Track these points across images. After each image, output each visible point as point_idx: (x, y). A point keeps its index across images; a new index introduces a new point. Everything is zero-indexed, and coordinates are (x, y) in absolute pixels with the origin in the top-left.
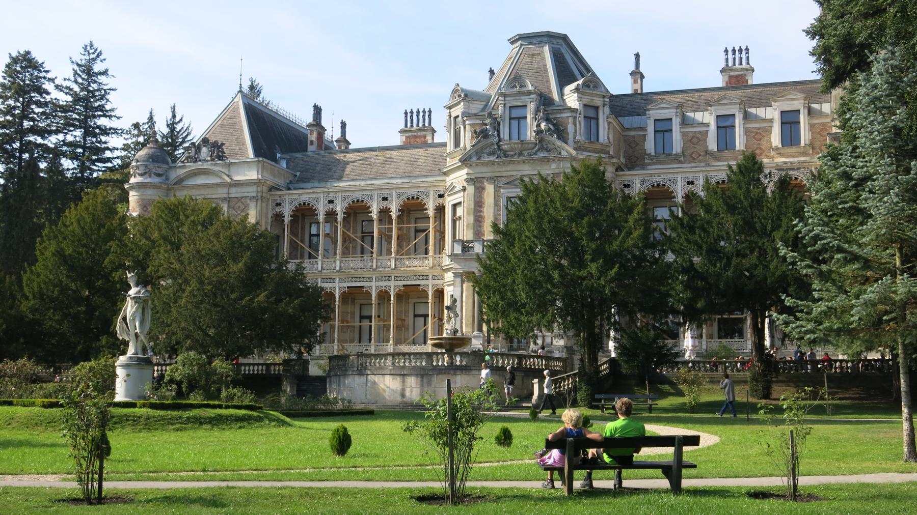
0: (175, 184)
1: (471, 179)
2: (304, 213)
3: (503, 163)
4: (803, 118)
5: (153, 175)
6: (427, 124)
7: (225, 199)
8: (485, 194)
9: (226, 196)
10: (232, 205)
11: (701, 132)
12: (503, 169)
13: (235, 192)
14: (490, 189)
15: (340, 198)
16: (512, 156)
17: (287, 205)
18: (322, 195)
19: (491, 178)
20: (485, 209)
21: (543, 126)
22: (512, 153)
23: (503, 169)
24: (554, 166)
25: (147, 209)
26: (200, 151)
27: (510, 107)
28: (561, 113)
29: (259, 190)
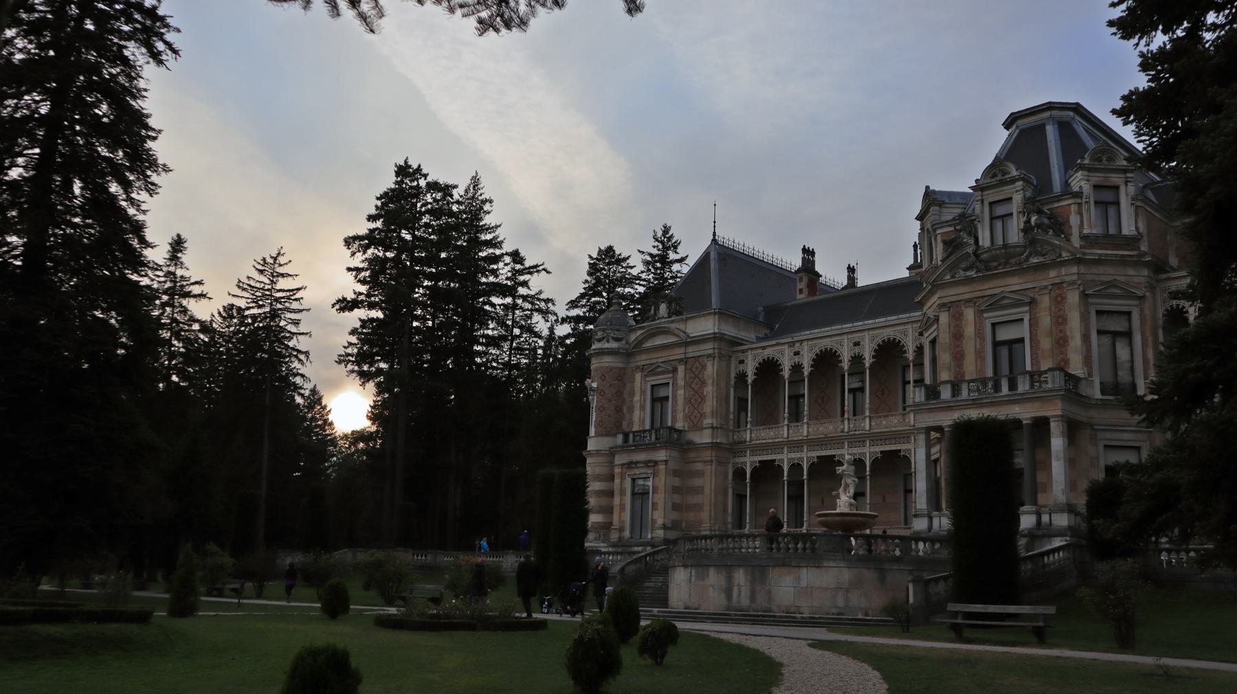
2: (769, 369)
7: (681, 360)
9: (683, 356)
10: (689, 366)
12: (986, 287)
13: (692, 351)
14: (969, 314)
15: (806, 347)
16: (996, 268)
19: (969, 301)
21: (1033, 219)
22: (995, 264)
23: (986, 287)
24: (1053, 273)
25: (605, 377)
27: (991, 204)
29: (716, 347)
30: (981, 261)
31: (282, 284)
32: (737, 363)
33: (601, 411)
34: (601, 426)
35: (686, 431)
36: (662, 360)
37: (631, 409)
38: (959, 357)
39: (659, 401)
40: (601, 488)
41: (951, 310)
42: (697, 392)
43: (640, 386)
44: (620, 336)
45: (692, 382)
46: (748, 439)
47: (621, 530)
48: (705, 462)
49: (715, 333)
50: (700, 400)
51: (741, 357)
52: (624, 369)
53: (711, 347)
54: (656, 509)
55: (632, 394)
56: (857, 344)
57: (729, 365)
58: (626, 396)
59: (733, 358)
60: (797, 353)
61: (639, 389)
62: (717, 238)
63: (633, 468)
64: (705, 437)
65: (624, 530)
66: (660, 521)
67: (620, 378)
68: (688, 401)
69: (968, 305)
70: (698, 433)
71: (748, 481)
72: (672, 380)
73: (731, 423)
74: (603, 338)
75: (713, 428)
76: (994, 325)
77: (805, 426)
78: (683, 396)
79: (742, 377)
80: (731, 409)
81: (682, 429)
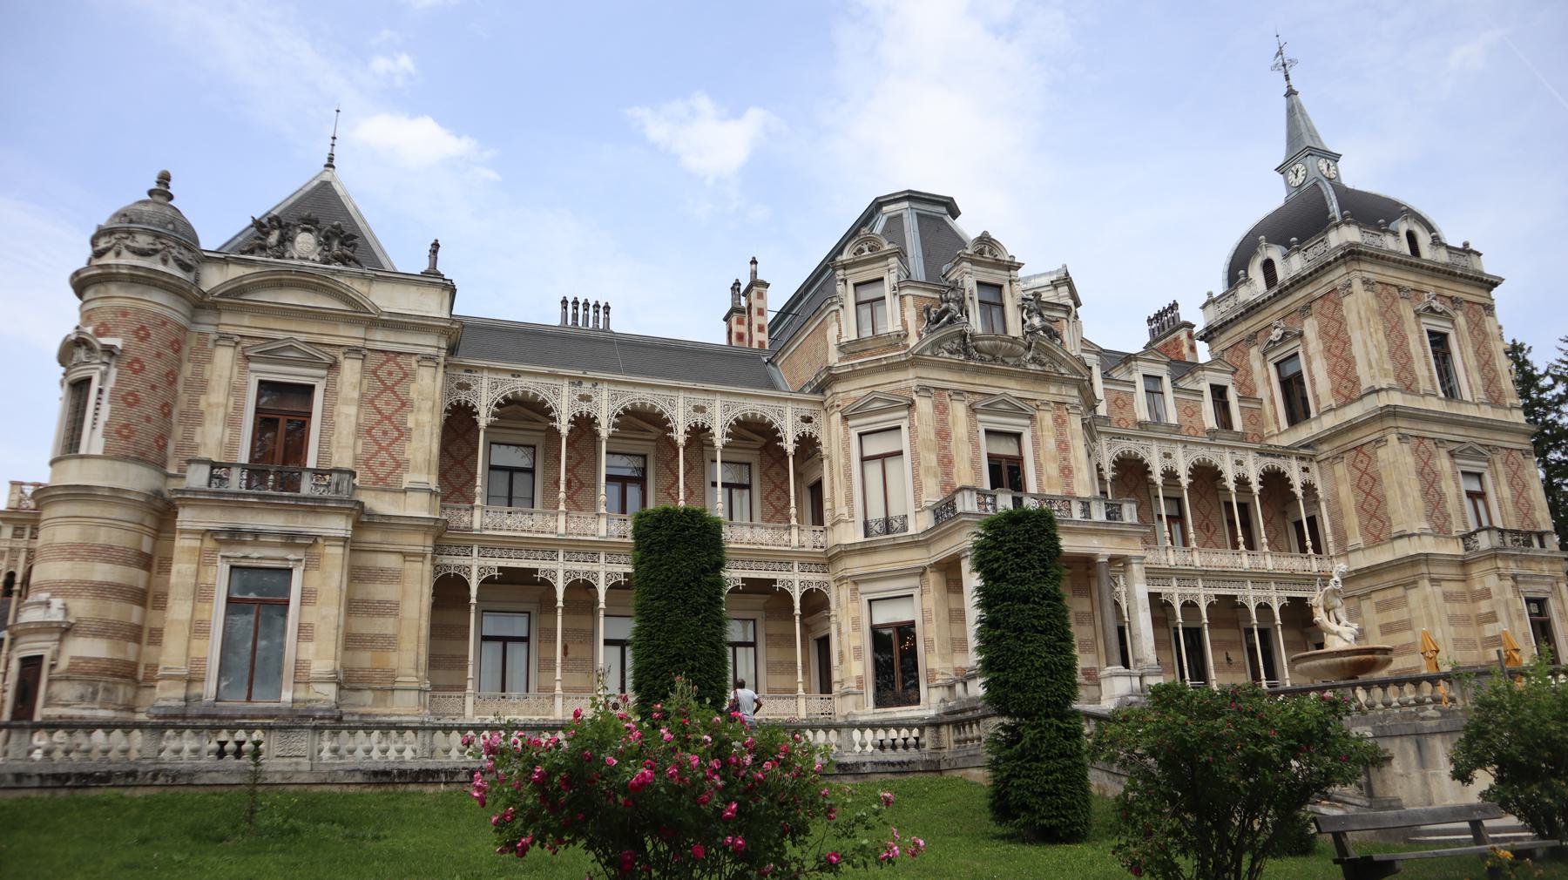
0: (221, 296)
1: (926, 389)
3: (977, 371)
4: (1232, 396)
5: (171, 261)
6: (601, 327)
7: (357, 350)
8: (950, 418)
9: (360, 343)
11: (1126, 393)
17: (484, 391)
19: (959, 393)
24: (1053, 390)
25: (148, 335)
26: (292, 240)
28: (1052, 310)
30: (975, 348)
33: (130, 405)
34: (127, 437)
36: (303, 338)
37: (195, 418)
38: (946, 462)
40: (110, 578)
42: (389, 418)
48: (404, 555)
50: (396, 434)
51: (465, 377)
52: (184, 329)
54: (309, 639)
55: (202, 386)
56: (700, 409)
58: (180, 387)
60: (585, 398)
61: (225, 382)
63: (244, 543)
64: (418, 507)
65: (202, 680)
68: (364, 431)
69: (955, 397)
70: (387, 497)
74: (156, 251)
77: (562, 518)
78: (353, 419)
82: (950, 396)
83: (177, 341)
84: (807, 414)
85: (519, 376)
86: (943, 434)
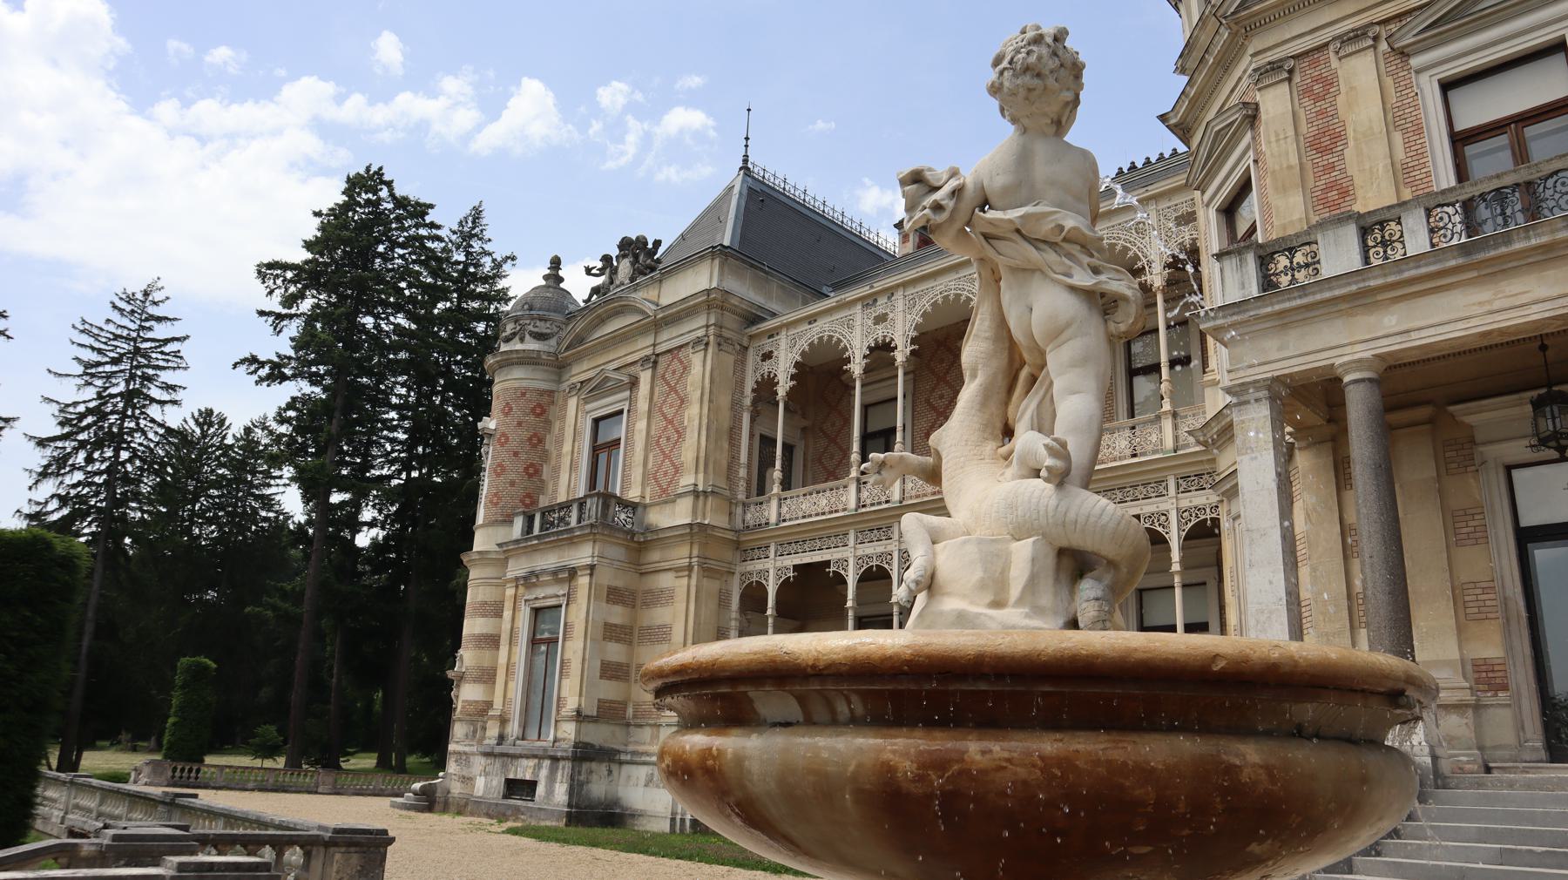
1: (1275, 67)
5: (527, 337)
7: (646, 359)
8: (1341, 100)
9: (649, 351)
18: (859, 307)
19: (1357, 35)
20: (1349, 153)
25: (511, 409)
29: (712, 321)
31: (160, 331)
32: (759, 359)
34: (496, 504)
35: (645, 506)
39: (603, 449)
41: (1297, 79)
43: (574, 419)
44: (548, 331)
45: (665, 401)
46: (773, 519)
47: (503, 721)
48: (677, 570)
49: (708, 292)
52: (551, 393)
53: (703, 323)
57: (741, 363)
59: (751, 352)
62: (750, 166)
64: (679, 515)
66: (571, 703)
67: (542, 409)
71: (769, 612)
72: (627, 403)
73: (742, 485)
74: (514, 334)
75: (696, 494)
76: (1447, 86)
79: (766, 387)
80: (743, 458)
81: (637, 500)
82: (1337, 53)
83: (539, 405)
84: (1184, 209)
85: (815, 321)
86: (1326, 141)
